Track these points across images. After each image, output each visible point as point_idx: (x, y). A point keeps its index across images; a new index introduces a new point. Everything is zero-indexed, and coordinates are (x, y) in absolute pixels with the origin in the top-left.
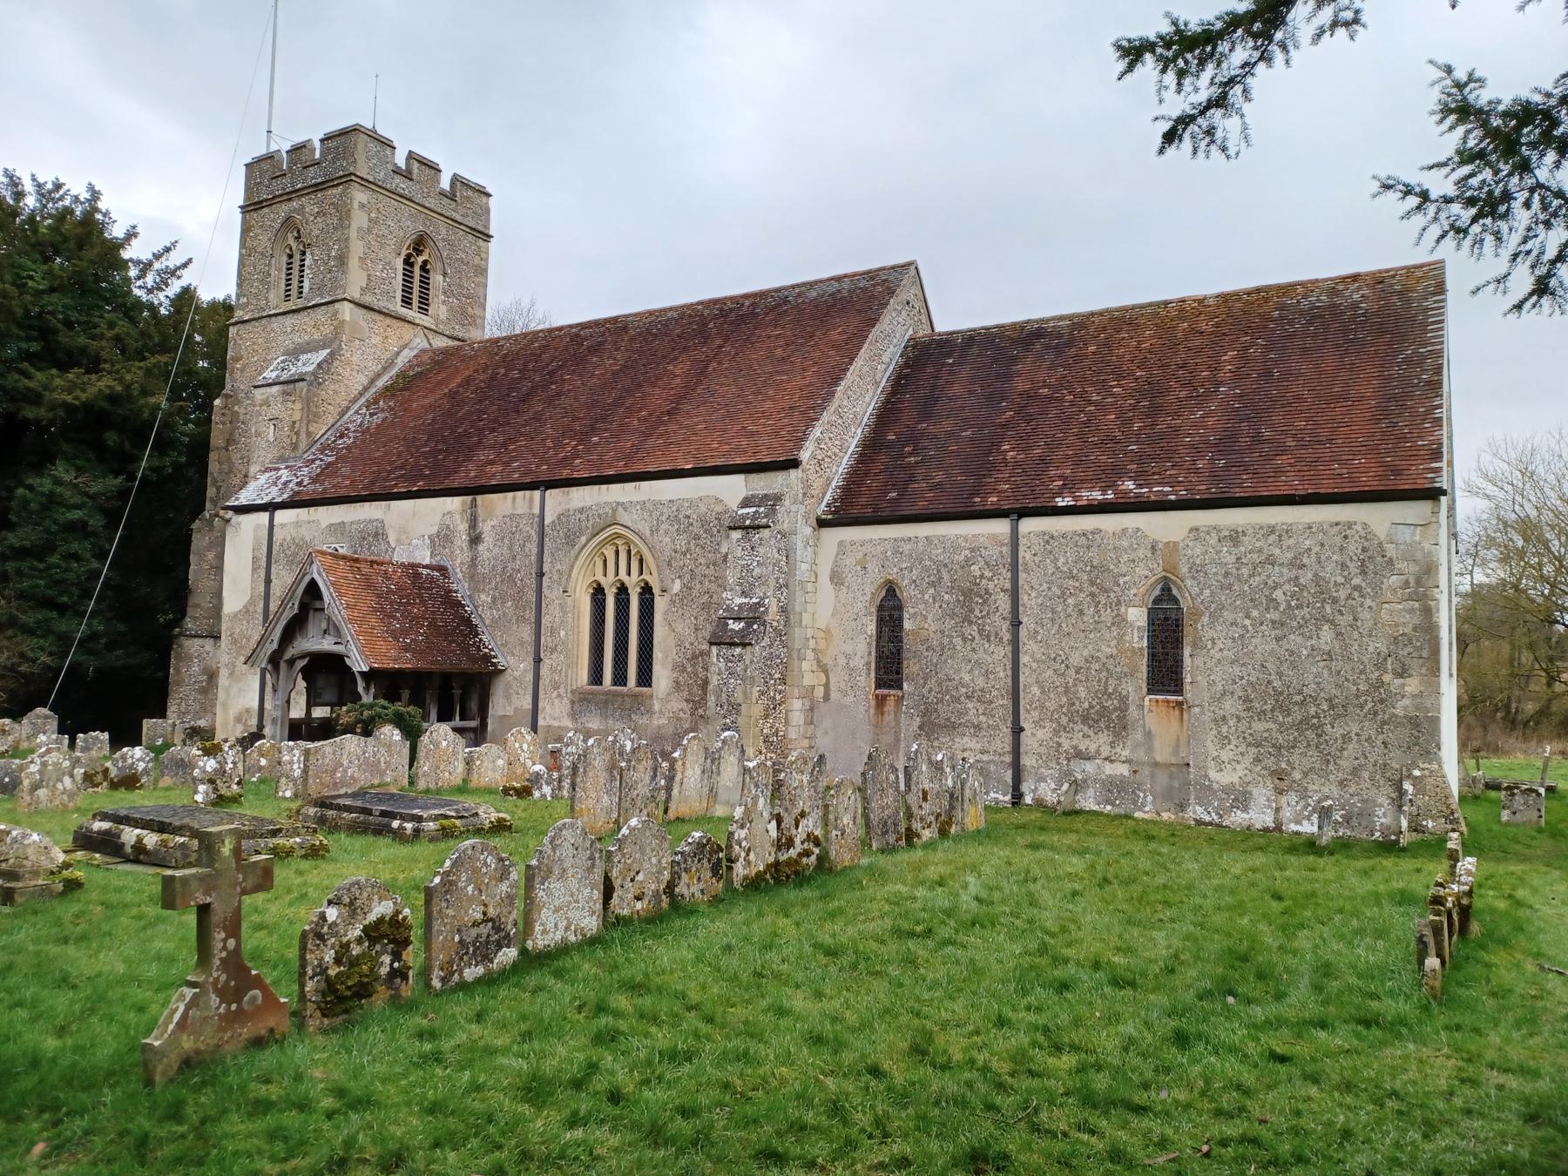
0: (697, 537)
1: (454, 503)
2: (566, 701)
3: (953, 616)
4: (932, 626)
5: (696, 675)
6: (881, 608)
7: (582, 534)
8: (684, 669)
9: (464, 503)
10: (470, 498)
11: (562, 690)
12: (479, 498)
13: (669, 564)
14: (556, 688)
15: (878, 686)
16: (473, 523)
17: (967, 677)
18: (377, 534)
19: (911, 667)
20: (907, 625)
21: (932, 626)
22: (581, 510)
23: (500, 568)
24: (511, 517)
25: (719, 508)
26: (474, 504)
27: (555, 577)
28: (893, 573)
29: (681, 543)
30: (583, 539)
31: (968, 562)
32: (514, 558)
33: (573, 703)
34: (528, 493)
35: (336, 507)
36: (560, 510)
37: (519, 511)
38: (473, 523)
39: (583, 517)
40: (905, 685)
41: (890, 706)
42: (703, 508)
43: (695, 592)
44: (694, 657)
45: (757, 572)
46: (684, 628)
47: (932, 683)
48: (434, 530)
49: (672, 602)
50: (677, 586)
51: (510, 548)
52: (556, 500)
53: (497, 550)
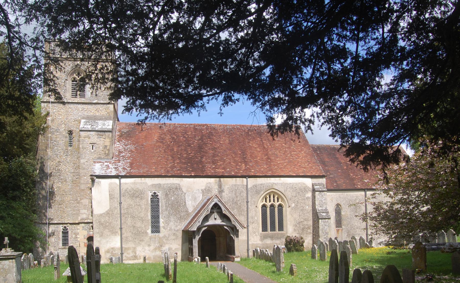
0: (299, 193)
1: (213, 180)
2: (258, 236)
3: (353, 211)
4: (348, 213)
5: (300, 227)
6: (336, 210)
7: (261, 191)
8: (296, 226)
9: (215, 180)
10: (218, 179)
11: (257, 234)
12: (222, 179)
13: (290, 199)
14: (254, 233)
15: (336, 227)
16: (220, 186)
17: (357, 224)
18: (176, 188)
19: (344, 222)
20: (343, 213)
21: (348, 213)
22: (261, 184)
23: (231, 200)
24: (235, 185)
25: (304, 186)
26: (220, 181)
27: (253, 202)
28: (339, 202)
29: (294, 194)
30: (262, 192)
31: (356, 200)
32: (237, 197)
33: (261, 237)
34: (241, 179)
35: (156, 179)
36: (254, 184)
37: (238, 184)
38: (220, 186)
39: (262, 186)
40: (343, 227)
41: (340, 231)
42: (300, 186)
43: (299, 207)
44: (299, 223)
45: (324, 201)
46: (296, 216)
47: (349, 226)
48: (203, 188)
49: (292, 209)
50: (293, 205)
51: (236, 194)
52: (251, 182)
53: (230, 195)
